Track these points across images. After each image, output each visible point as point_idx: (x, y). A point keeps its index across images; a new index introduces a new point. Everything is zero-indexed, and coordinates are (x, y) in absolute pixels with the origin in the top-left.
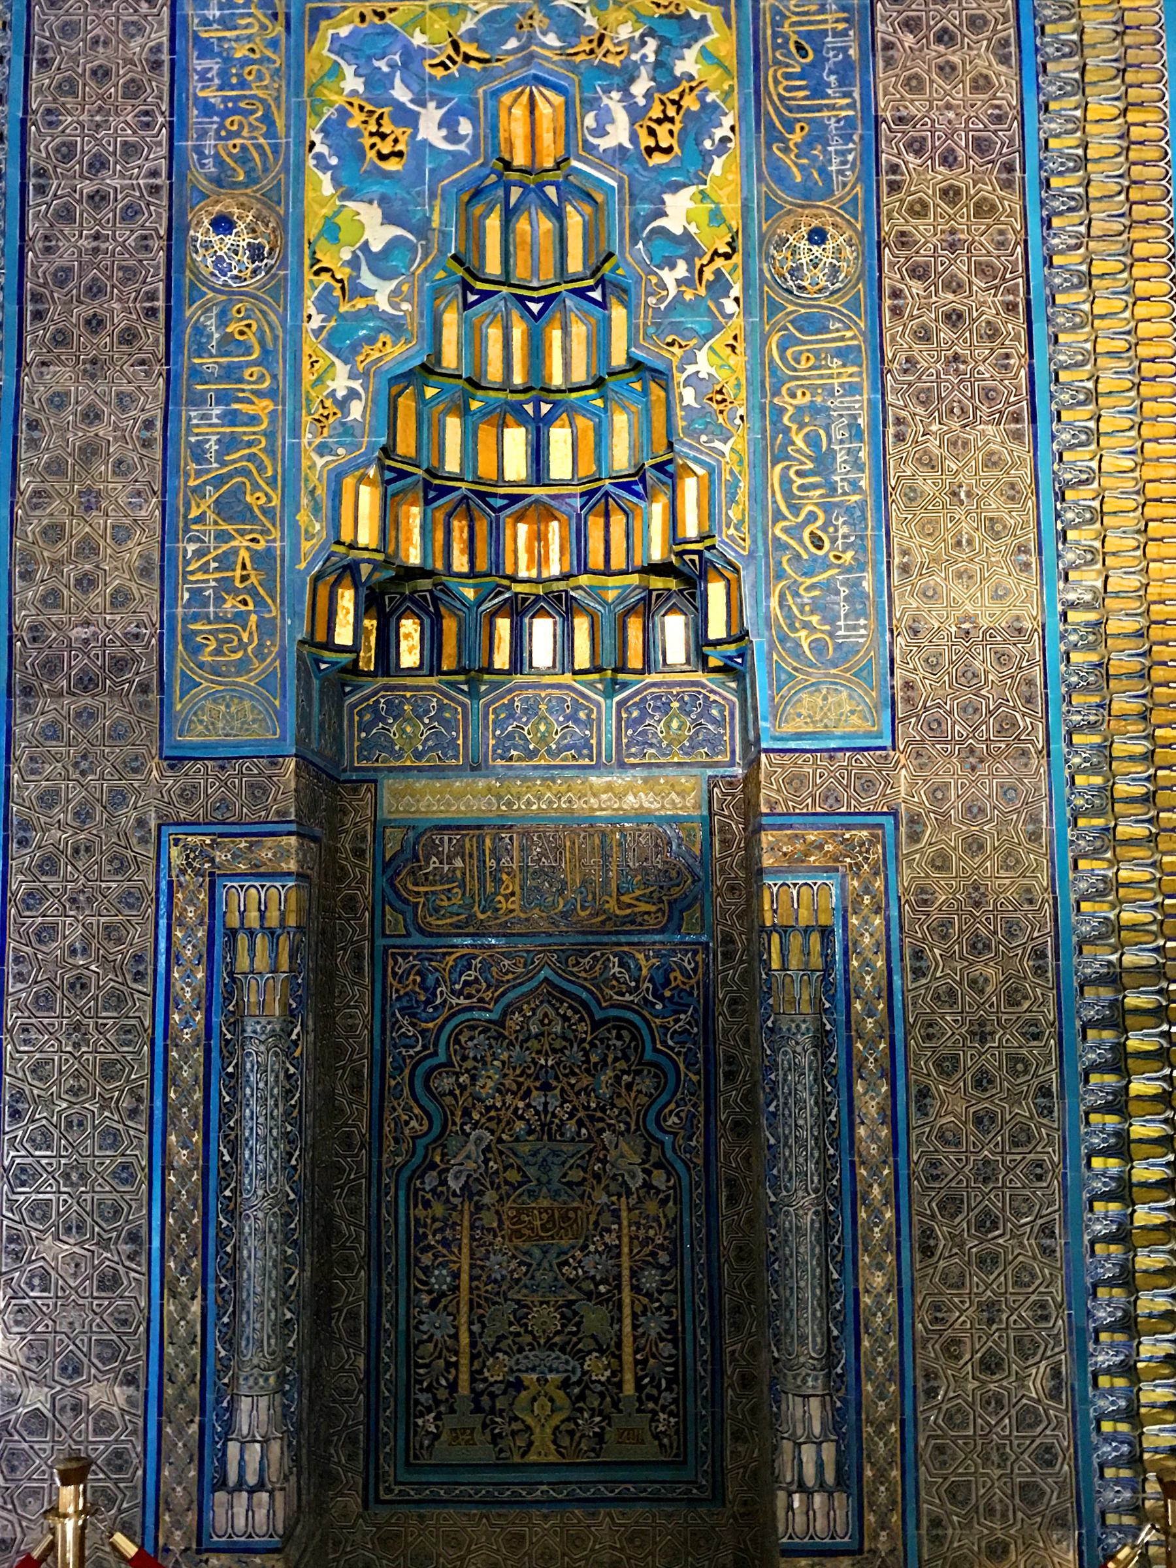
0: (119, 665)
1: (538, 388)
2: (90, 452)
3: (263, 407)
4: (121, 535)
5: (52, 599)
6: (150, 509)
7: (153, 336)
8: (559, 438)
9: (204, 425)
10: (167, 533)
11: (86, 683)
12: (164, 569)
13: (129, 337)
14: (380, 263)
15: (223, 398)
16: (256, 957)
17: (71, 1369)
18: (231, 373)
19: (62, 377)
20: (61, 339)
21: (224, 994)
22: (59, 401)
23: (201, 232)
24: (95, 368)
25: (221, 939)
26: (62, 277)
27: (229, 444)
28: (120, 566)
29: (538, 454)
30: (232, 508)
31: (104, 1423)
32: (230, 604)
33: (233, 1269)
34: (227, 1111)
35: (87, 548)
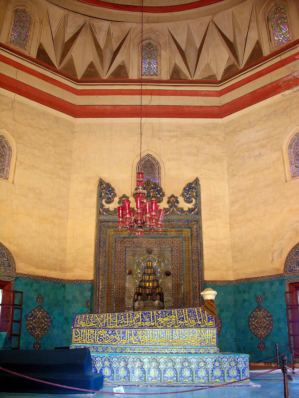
1: (149, 280)
8: (151, 283)
14: (139, 273)
29: (149, 284)
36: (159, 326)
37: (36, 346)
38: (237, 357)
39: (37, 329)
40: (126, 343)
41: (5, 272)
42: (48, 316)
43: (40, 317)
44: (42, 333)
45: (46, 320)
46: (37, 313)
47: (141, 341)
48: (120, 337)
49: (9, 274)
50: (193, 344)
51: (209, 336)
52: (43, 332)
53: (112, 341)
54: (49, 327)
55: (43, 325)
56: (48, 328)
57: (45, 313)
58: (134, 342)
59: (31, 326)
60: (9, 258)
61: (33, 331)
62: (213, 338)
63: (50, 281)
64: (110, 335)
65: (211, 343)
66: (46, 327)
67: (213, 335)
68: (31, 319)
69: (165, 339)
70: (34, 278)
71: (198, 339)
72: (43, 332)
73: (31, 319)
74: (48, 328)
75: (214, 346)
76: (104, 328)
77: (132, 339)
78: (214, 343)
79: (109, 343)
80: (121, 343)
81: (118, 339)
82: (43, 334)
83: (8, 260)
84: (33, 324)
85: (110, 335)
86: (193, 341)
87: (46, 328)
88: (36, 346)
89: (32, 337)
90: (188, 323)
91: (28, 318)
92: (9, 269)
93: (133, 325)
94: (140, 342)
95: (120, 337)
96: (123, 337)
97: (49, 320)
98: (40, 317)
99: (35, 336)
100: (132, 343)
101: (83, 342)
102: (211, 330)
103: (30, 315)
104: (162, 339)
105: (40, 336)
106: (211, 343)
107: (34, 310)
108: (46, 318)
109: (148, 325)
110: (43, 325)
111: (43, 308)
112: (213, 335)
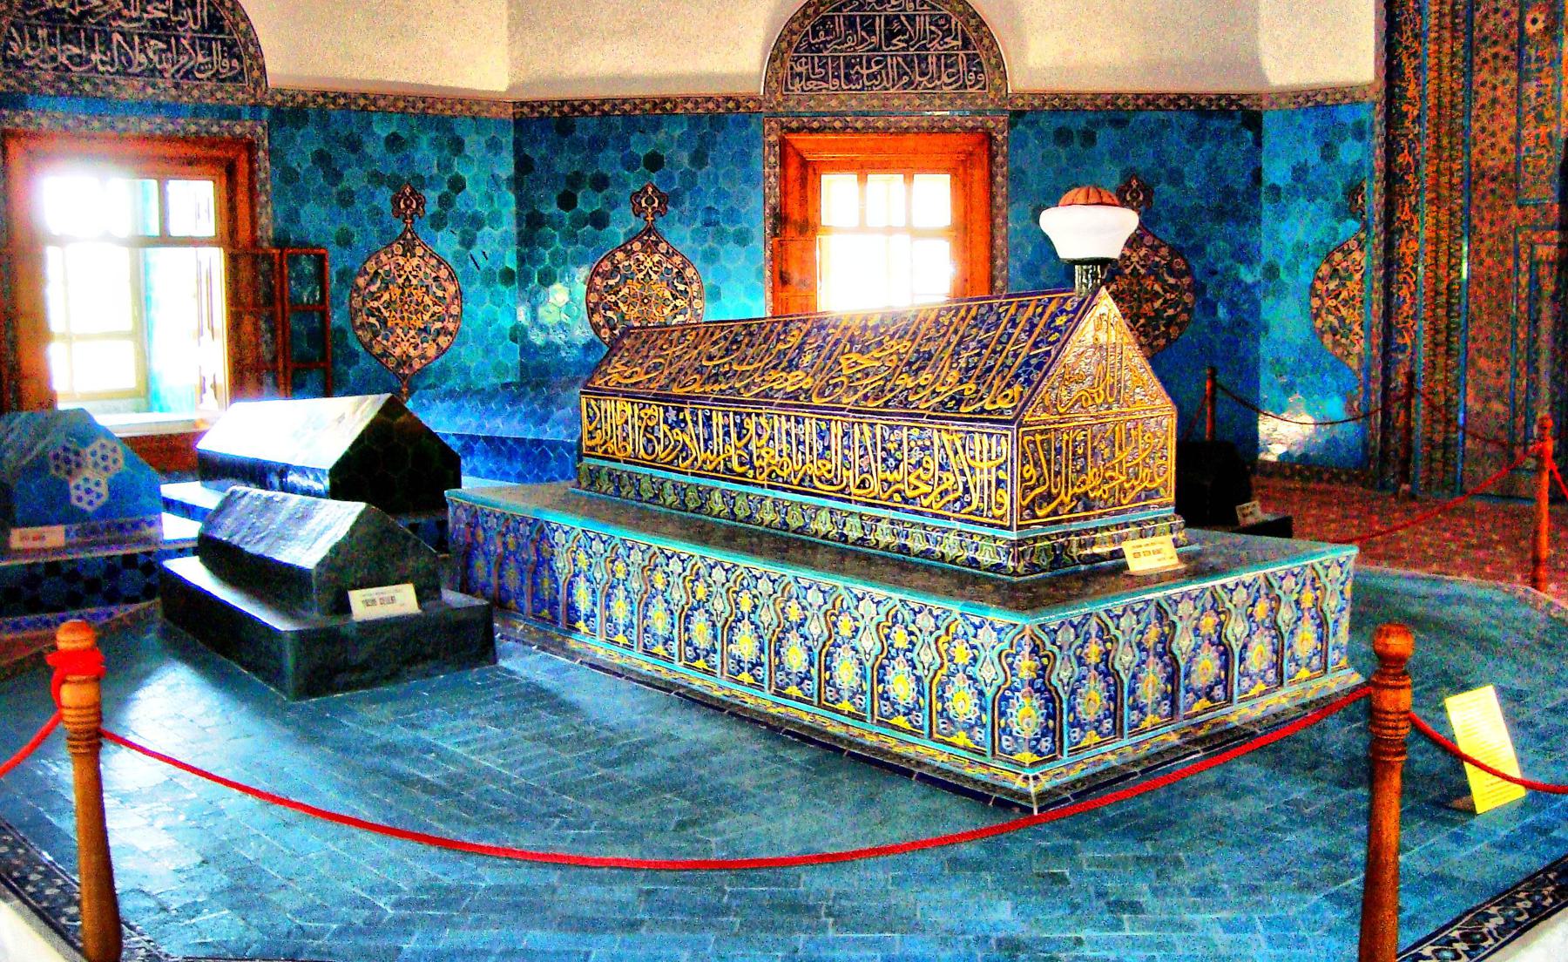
0: (1503, 173)
2: (1494, 101)
3: (1550, 81)
4: (1504, 129)
5: (1482, 152)
6: (1514, 120)
7: (1513, 56)
9: (1531, 89)
10: (1520, 126)
11: (1494, 179)
12: (1517, 140)
13: (1506, 59)
15: (1538, 79)
16: (1544, 271)
17: (1488, 399)
18: (1540, 70)
19: (1485, 74)
20: (1485, 62)
21: (1535, 282)
22: (1483, 84)
23: (1528, 25)
24: (1496, 71)
25: (1534, 264)
26: (1485, 39)
27: (1539, 94)
28: (1503, 140)
30: (1539, 118)
31: (1497, 415)
32: (1538, 151)
33: (1537, 371)
34: (1536, 321)
35: (1493, 135)
36: (821, 394)
38: (977, 621)
40: (715, 470)
41: (961, 96)
42: (1179, 264)
43: (1142, 271)
44: (1156, 338)
45: (1172, 281)
47: (757, 464)
48: (697, 436)
49: (979, 102)
50: (926, 502)
51: (982, 471)
53: (677, 457)
54: (1187, 310)
55: (1157, 304)
56: (1184, 317)
57: (1164, 251)
58: (735, 465)
60: (972, 36)
62: (999, 482)
63: (1180, 108)
64: (672, 428)
65: (989, 509)
66: (1170, 312)
67: (998, 468)
69: (829, 466)
70: (1099, 102)
71: (940, 479)
74: (1184, 317)
75: (1002, 527)
76: (657, 397)
77: (732, 451)
78: (998, 513)
79: (671, 463)
80: (701, 468)
81: (693, 446)
82: (1162, 342)
83: (966, 43)
85: (672, 428)
86: (925, 488)
90: (924, 387)
92: (978, 82)
93: (745, 387)
94: (755, 468)
95: (697, 436)
96: (706, 441)
97: (1186, 280)
98: (1142, 271)
100: (731, 471)
101: (606, 451)
102: (990, 435)
104: (820, 462)
106: (989, 509)
108: (1172, 273)
109: (789, 389)
112: (998, 468)
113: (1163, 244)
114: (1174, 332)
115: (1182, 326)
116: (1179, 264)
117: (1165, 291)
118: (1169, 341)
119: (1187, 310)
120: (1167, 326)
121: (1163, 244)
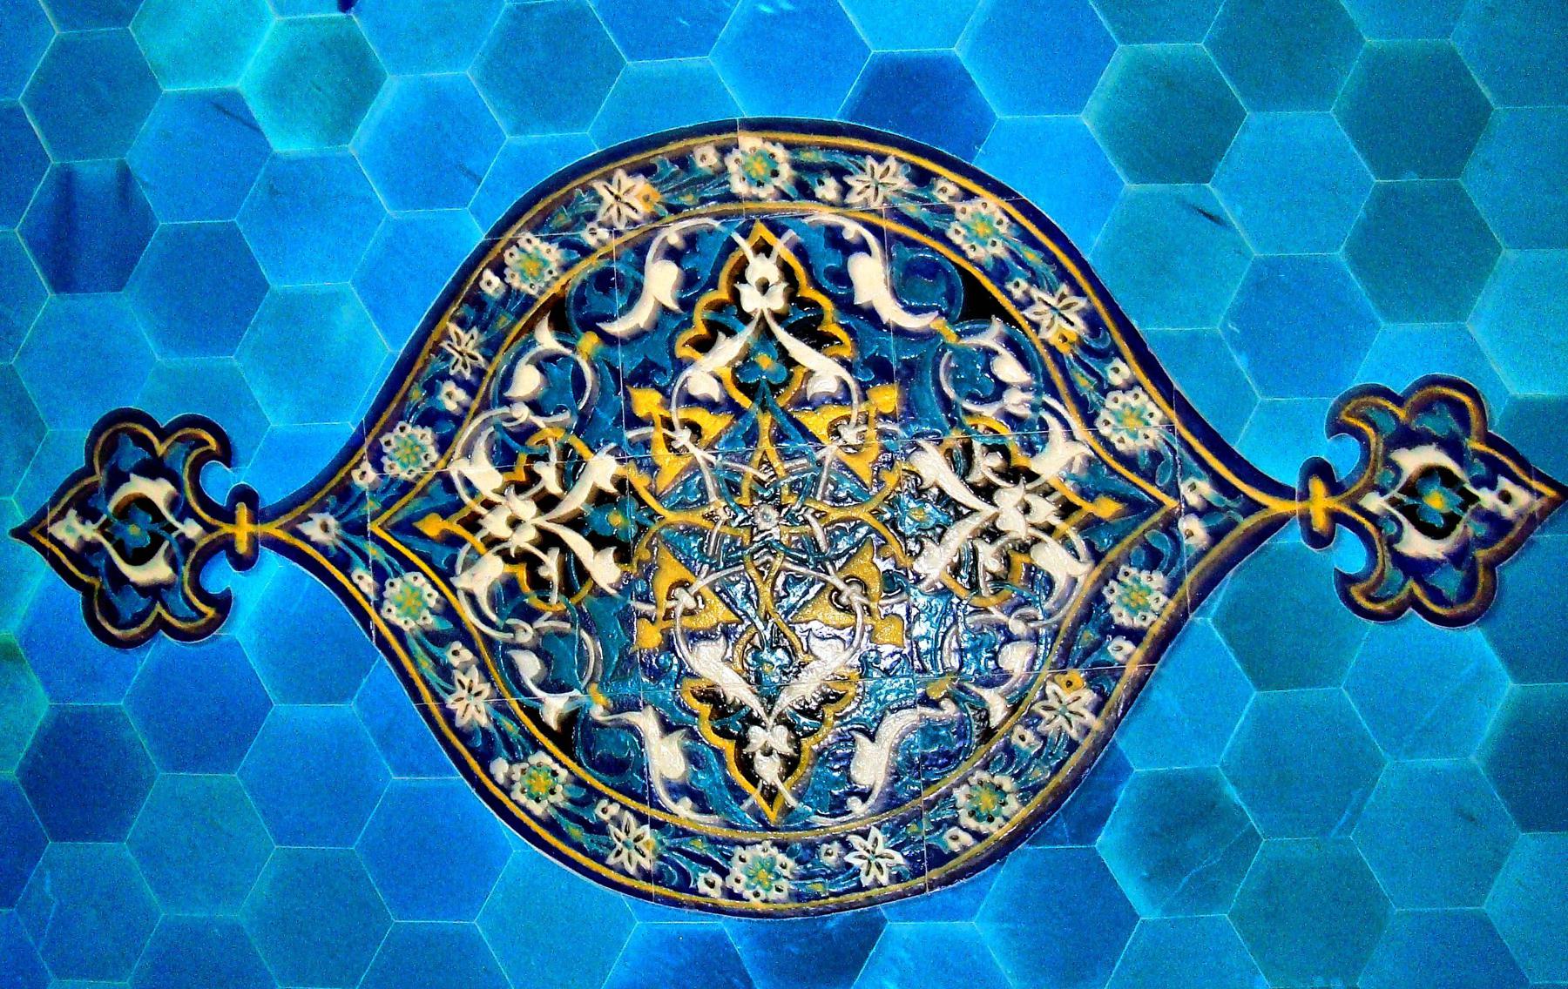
37: (159, 491)
39: (602, 470)
44: (496, 659)
45: (872, 765)
46: (1032, 433)
52: (529, 666)
56: (637, 849)
59: (662, 281)
61: (528, 381)
66: (665, 758)
68: (870, 279)
72: (529, 666)
73: (870, 279)
74: (637, 849)
84: (728, 350)
87: (623, 770)
88: (159, 491)
89: (385, 353)
91: (882, 181)
97: (878, 860)
99: (410, 450)
103: (980, 230)
105: (410, 601)
107: (1112, 331)
108: (927, 761)
110: (712, 664)
111: (1203, 621)
113: (1121, 701)
114: (541, 782)
115: (571, 834)
116: (984, 805)
117: (727, 318)
118: (485, 747)
119: (670, 881)
120: (572, 734)
121: (1121, 701)
